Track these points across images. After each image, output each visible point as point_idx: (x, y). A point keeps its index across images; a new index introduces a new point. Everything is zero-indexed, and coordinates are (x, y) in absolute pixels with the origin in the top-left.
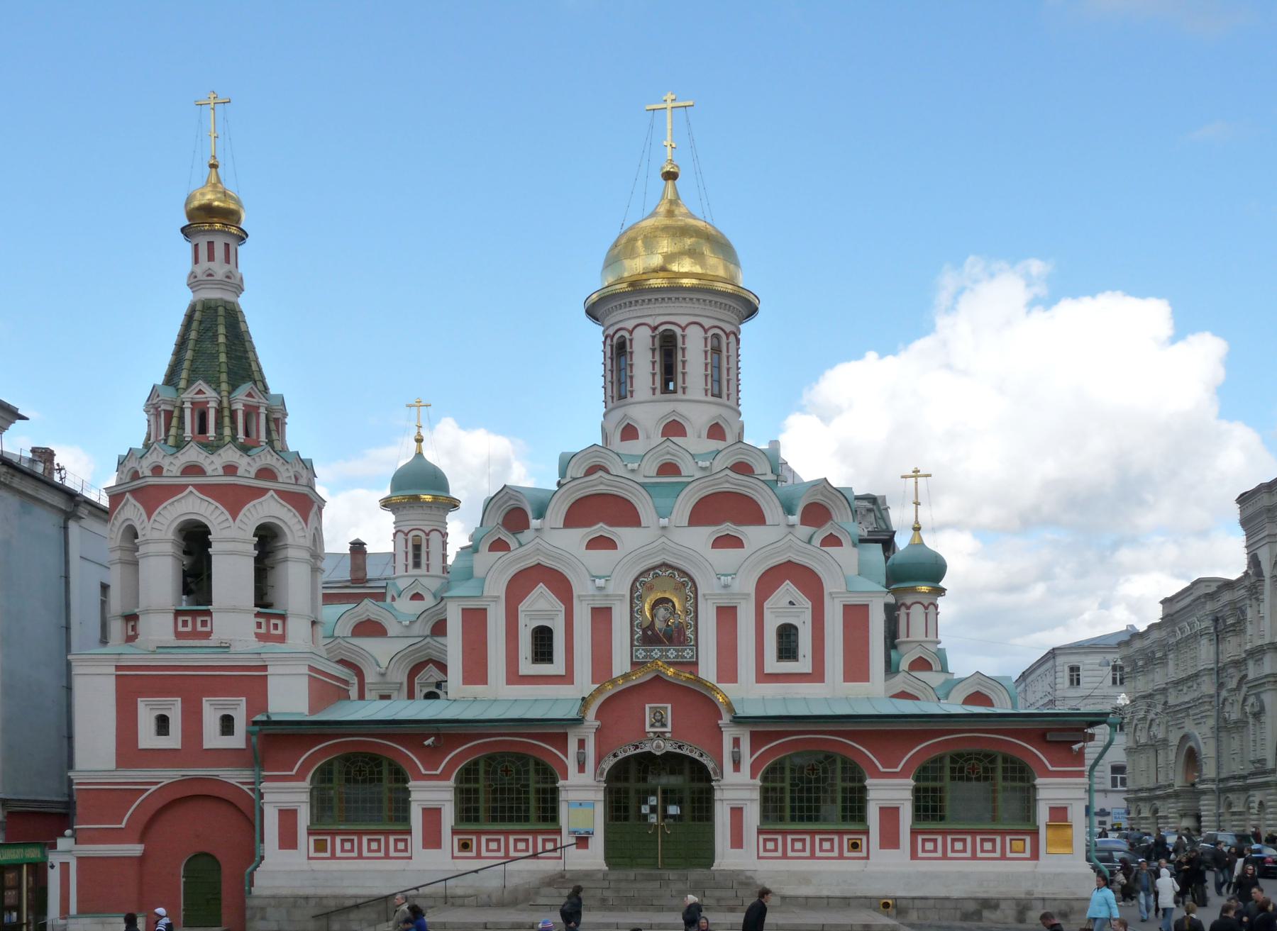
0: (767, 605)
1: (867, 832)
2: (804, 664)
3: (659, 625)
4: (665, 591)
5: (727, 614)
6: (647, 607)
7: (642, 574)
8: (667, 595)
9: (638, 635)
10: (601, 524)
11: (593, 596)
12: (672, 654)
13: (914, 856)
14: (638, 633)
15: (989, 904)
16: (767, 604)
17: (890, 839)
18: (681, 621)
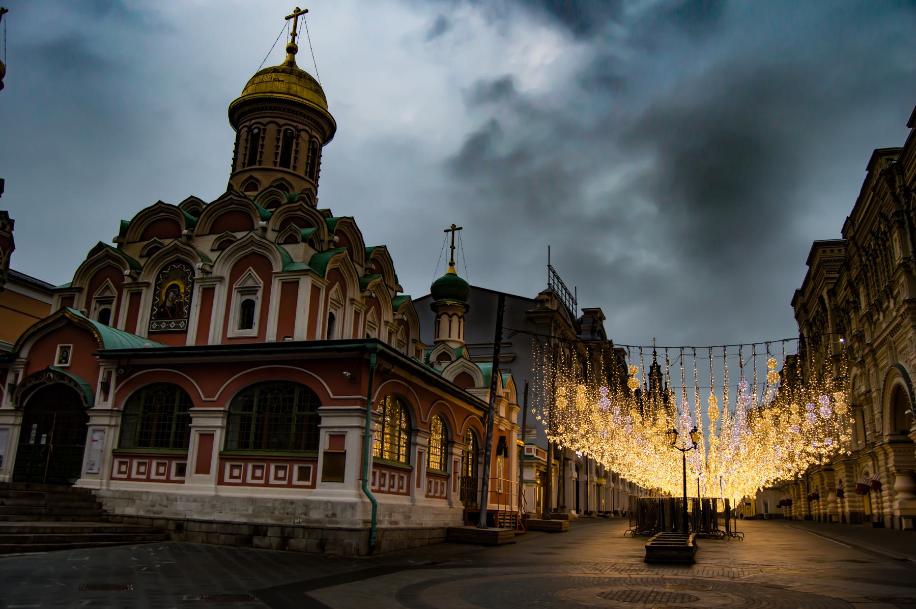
0: (234, 287)
1: (185, 457)
2: (253, 332)
3: (168, 304)
4: (175, 280)
5: (208, 295)
6: (164, 291)
7: (165, 268)
8: (175, 282)
9: (155, 312)
10: (155, 238)
11: (129, 284)
12: (173, 325)
13: (221, 481)
14: (155, 310)
15: (259, 530)
16: (236, 285)
17: (202, 468)
18: (181, 300)
